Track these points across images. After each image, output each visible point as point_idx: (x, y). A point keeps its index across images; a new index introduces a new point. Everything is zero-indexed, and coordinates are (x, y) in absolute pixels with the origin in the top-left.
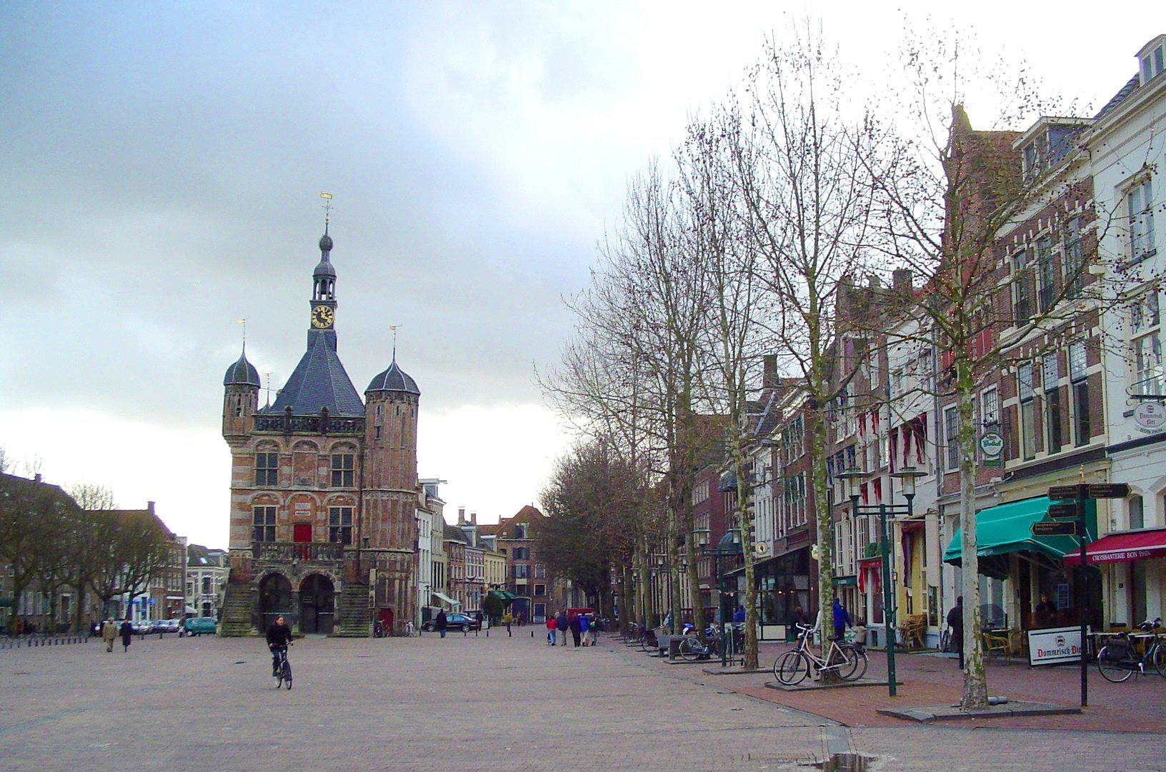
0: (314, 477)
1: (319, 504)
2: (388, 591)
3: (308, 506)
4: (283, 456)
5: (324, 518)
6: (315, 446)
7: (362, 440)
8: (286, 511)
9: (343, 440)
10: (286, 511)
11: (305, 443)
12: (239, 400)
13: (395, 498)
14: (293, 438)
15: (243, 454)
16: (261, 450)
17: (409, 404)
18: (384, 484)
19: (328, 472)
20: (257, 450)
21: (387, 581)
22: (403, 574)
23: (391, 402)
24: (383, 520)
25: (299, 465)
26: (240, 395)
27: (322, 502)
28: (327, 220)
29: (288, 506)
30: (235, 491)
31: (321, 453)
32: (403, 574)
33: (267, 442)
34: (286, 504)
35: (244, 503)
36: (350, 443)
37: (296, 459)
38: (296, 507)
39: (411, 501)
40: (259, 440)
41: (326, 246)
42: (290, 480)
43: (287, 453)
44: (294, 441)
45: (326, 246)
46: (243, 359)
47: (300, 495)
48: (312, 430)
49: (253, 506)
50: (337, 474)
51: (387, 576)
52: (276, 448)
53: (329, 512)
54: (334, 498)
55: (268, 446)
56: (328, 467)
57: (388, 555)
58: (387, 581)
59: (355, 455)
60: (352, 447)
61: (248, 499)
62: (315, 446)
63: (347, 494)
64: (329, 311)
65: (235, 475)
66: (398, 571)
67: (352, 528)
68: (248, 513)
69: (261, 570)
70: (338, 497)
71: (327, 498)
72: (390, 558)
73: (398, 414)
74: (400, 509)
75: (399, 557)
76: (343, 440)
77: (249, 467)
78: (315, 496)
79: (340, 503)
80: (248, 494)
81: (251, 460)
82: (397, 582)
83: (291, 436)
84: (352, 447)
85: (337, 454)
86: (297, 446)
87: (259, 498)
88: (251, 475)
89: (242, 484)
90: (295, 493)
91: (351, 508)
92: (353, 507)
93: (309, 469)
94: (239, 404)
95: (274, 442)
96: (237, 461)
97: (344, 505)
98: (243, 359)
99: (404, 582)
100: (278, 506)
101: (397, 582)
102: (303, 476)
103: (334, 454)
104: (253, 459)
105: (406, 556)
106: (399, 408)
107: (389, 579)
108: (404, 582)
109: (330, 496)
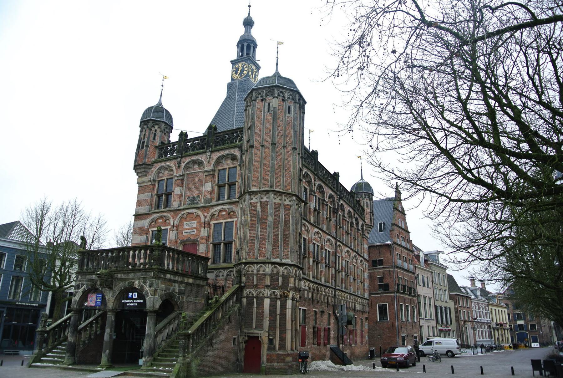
0: (202, 195)
1: (203, 220)
2: (257, 313)
3: (195, 224)
4: (176, 178)
5: (206, 235)
6: (200, 163)
7: (240, 147)
8: (175, 231)
9: (225, 152)
10: (175, 231)
11: (194, 162)
12: (145, 134)
13: (265, 199)
14: (184, 159)
15: (146, 182)
16: (162, 177)
17: (283, 100)
18: (254, 186)
19: (213, 188)
20: (158, 177)
21: (255, 300)
22: (278, 292)
23: (262, 100)
24: (251, 226)
25: (190, 186)
26: (146, 130)
27: (205, 218)
28: (249, 6)
29: (178, 227)
30: (138, 216)
31: (207, 168)
32: (278, 292)
33: (165, 168)
34: (175, 224)
35: (143, 227)
36: (232, 155)
37: (188, 178)
38: (185, 227)
39: (289, 203)
40: (158, 167)
41: (248, 23)
42: (180, 200)
43: (178, 175)
44: (186, 161)
45: (248, 23)
46: (160, 103)
47: (189, 213)
48: (200, 149)
49: (150, 230)
50: (220, 187)
51: (255, 294)
52: (172, 173)
53: (212, 228)
54: (217, 213)
55: (167, 172)
56: (213, 182)
57: (255, 268)
58: (255, 300)
59: (237, 164)
60: (234, 158)
61: (145, 223)
62: (200, 163)
63: (229, 206)
64: (245, 65)
65: (139, 203)
66: (268, 287)
67: (233, 242)
68: (145, 236)
69: (83, 285)
70: (221, 211)
71: (210, 214)
72: (258, 271)
73: (269, 111)
74: (270, 210)
75: (268, 269)
76: (225, 152)
77: (150, 194)
78: (200, 213)
79: (224, 217)
80: (146, 219)
81: (151, 187)
82: (267, 302)
83: (182, 158)
84: (234, 158)
85: (222, 168)
86: (187, 167)
87: (155, 221)
88: (151, 201)
89: (144, 209)
90: (182, 213)
91: (233, 221)
92: (235, 220)
93: (196, 188)
94: (144, 138)
95: (169, 166)
96: (142, 189)
97: (226, 218)
98: (160, 103)
99: (279, 302)
100: (169, 227)
101: (267, 302)
102: (193, 194)
103: (219, 168)
104: (154, 185)
105: (281, 269)
106: (271, 104)
108: (279, 302)
109: (213, 210)
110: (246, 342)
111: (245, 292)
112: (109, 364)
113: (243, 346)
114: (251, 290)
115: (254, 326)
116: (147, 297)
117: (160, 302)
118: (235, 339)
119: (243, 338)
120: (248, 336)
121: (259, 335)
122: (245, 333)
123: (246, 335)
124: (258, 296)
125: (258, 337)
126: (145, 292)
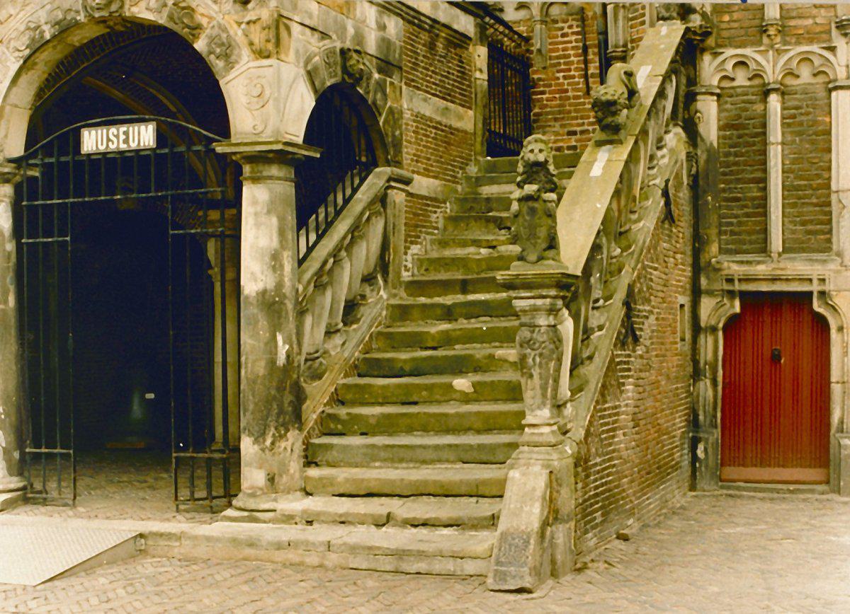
51: (772, 73)
107: (783, 93)
110: (733, 327)
111: (710, 72)
112: (16, 482)
113: (712, 348)
114: (748, 51)
115: (776, 242)
116: (230, 65)
117: (305, 102)
118: (682, 306)
119: (720, 305)
120: (743, 295)
121: (815, 287)
122: (730, 280)
123: (737, 287)
124: (790, 81)
125: (809, 295)
126: (212, 39)
